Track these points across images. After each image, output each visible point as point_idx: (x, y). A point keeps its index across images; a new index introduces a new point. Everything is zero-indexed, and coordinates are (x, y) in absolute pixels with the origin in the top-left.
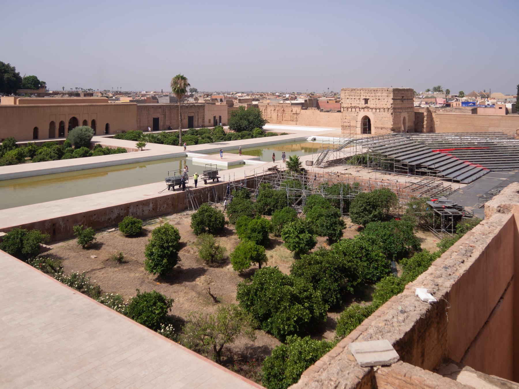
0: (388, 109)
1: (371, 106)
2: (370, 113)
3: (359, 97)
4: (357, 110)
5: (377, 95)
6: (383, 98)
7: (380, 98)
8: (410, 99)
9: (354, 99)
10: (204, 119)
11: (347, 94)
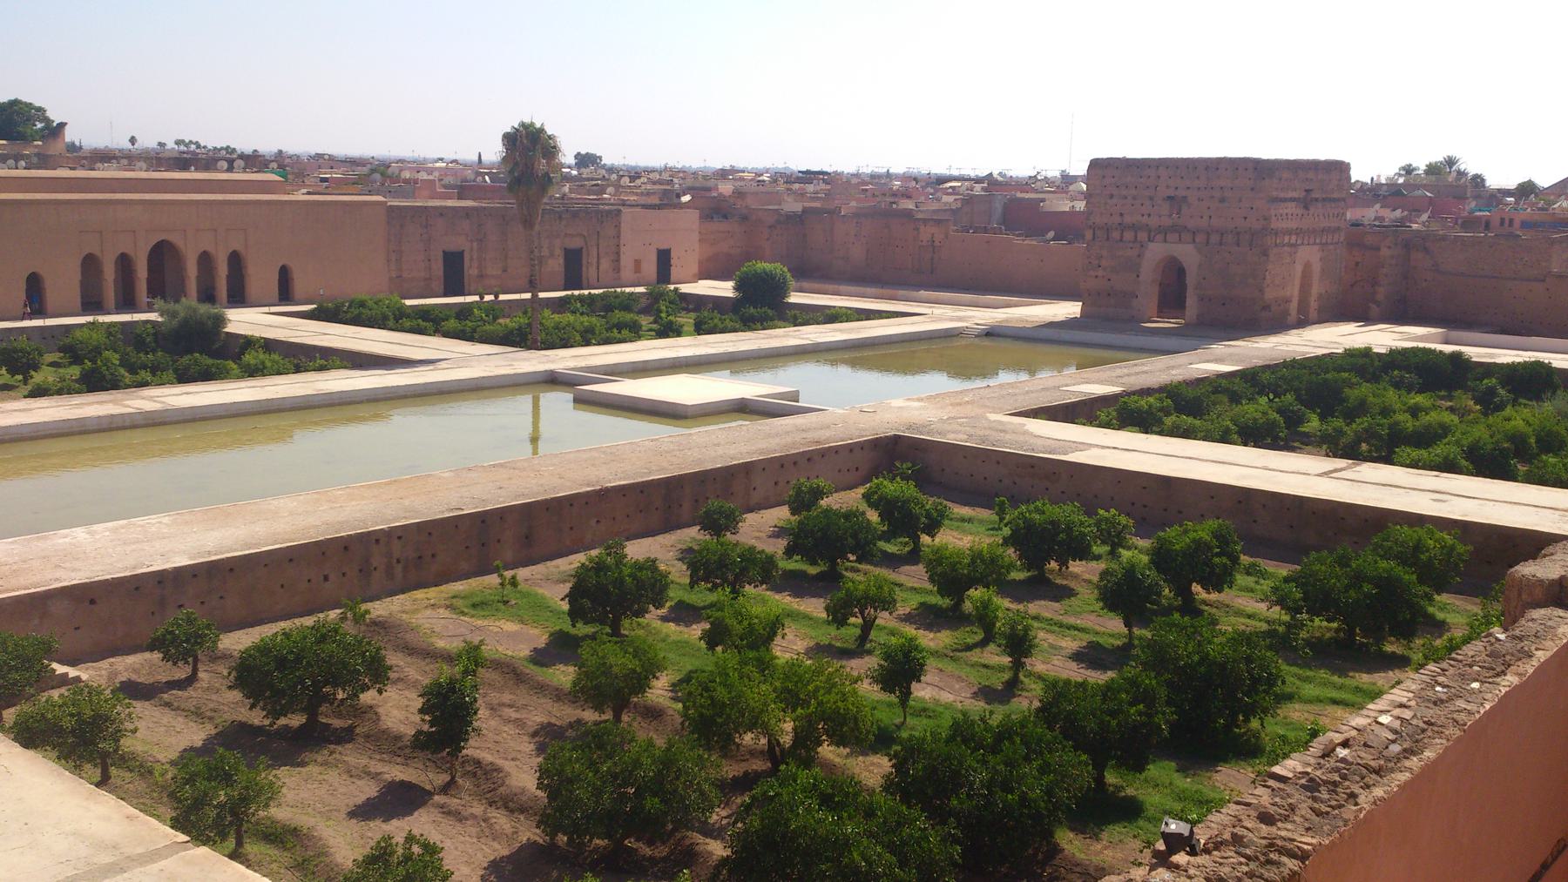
8: (1334, 200)
9: (1134, 198)
10: (618, 260)
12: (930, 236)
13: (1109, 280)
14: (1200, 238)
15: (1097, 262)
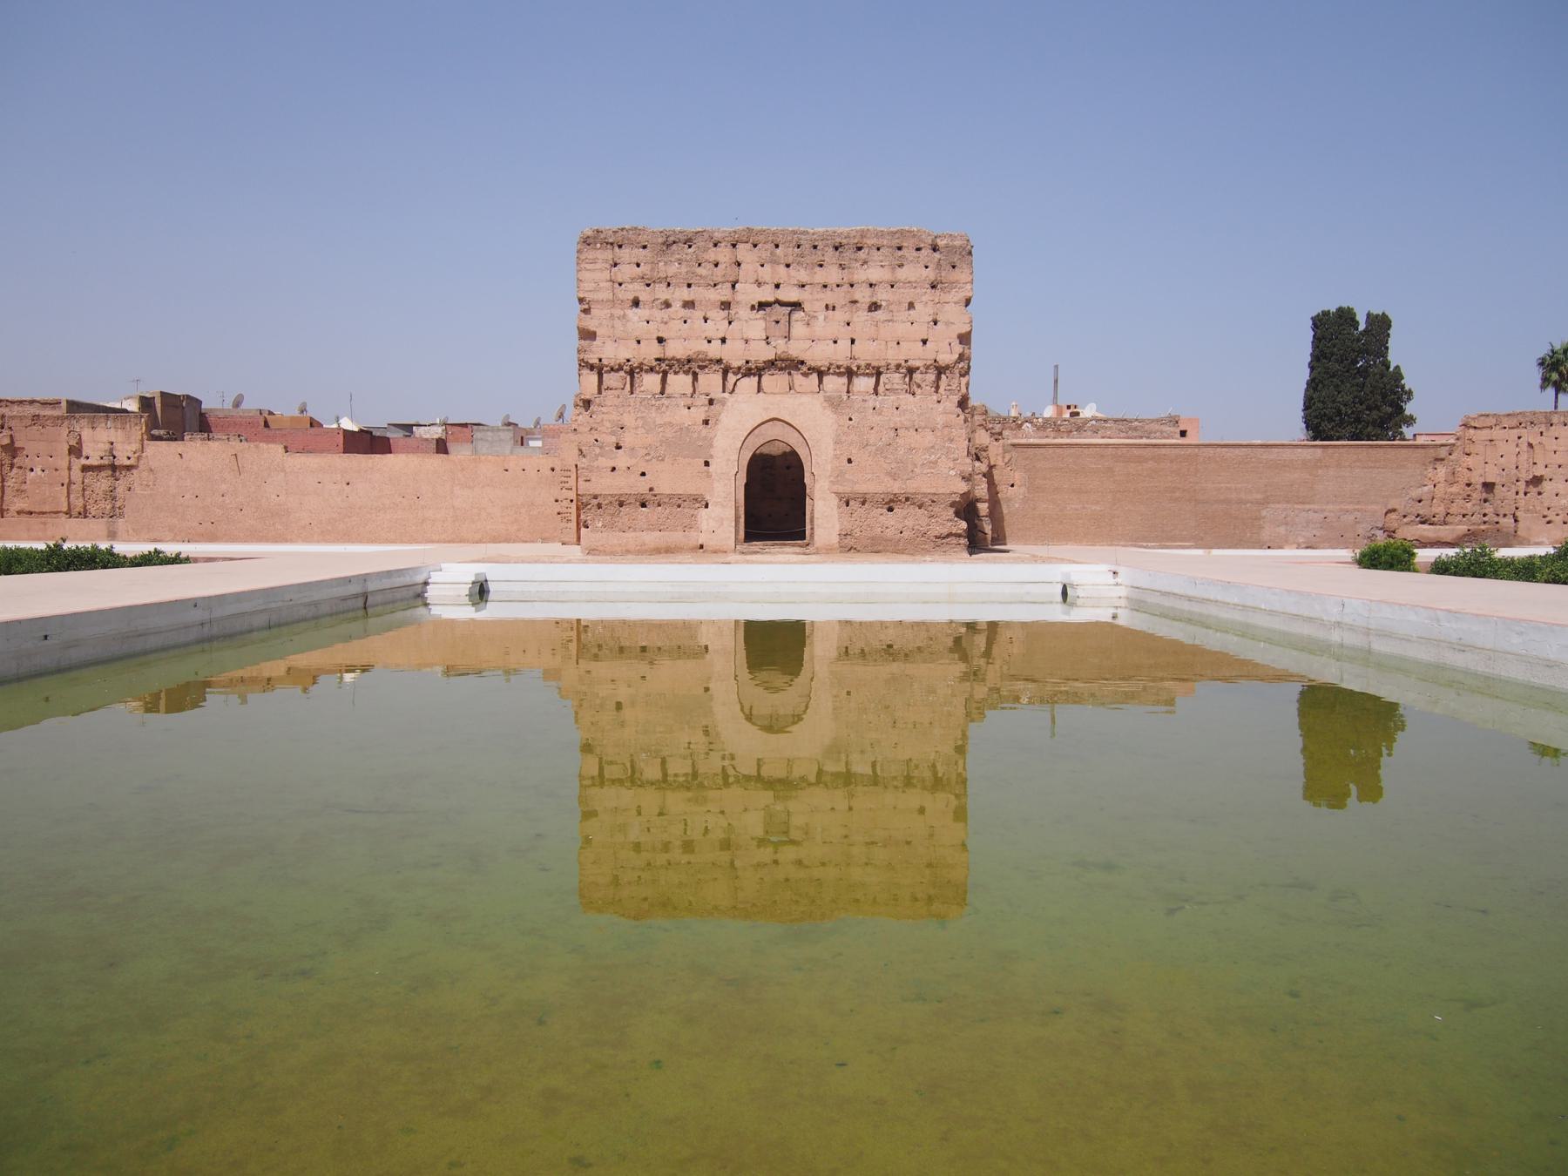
0: (940, 370)
1: (819, 354)
2: (805, 399)
3: (724, 293)
4: (710, 381)
5: (862, 275)
6: (907, 294)
7: (882, 295)
9: (689, 305)
11: (626, 271)
12: (108, 446)
13: (643, 474)
14: (834, 383)
15: (613, 439)
